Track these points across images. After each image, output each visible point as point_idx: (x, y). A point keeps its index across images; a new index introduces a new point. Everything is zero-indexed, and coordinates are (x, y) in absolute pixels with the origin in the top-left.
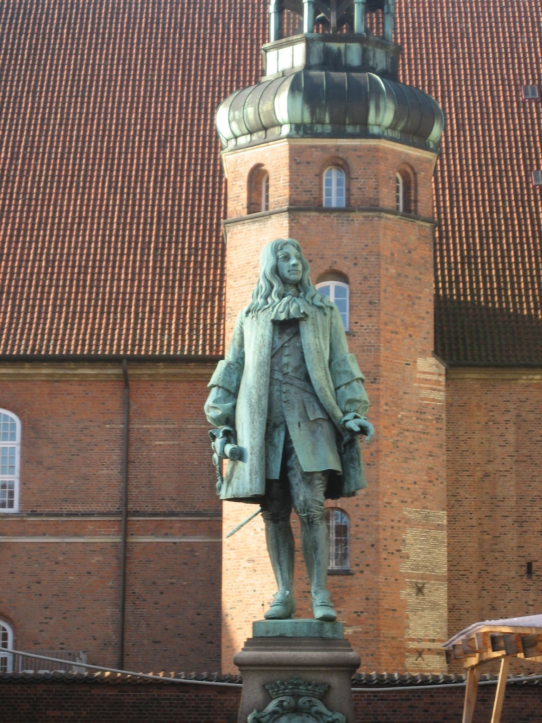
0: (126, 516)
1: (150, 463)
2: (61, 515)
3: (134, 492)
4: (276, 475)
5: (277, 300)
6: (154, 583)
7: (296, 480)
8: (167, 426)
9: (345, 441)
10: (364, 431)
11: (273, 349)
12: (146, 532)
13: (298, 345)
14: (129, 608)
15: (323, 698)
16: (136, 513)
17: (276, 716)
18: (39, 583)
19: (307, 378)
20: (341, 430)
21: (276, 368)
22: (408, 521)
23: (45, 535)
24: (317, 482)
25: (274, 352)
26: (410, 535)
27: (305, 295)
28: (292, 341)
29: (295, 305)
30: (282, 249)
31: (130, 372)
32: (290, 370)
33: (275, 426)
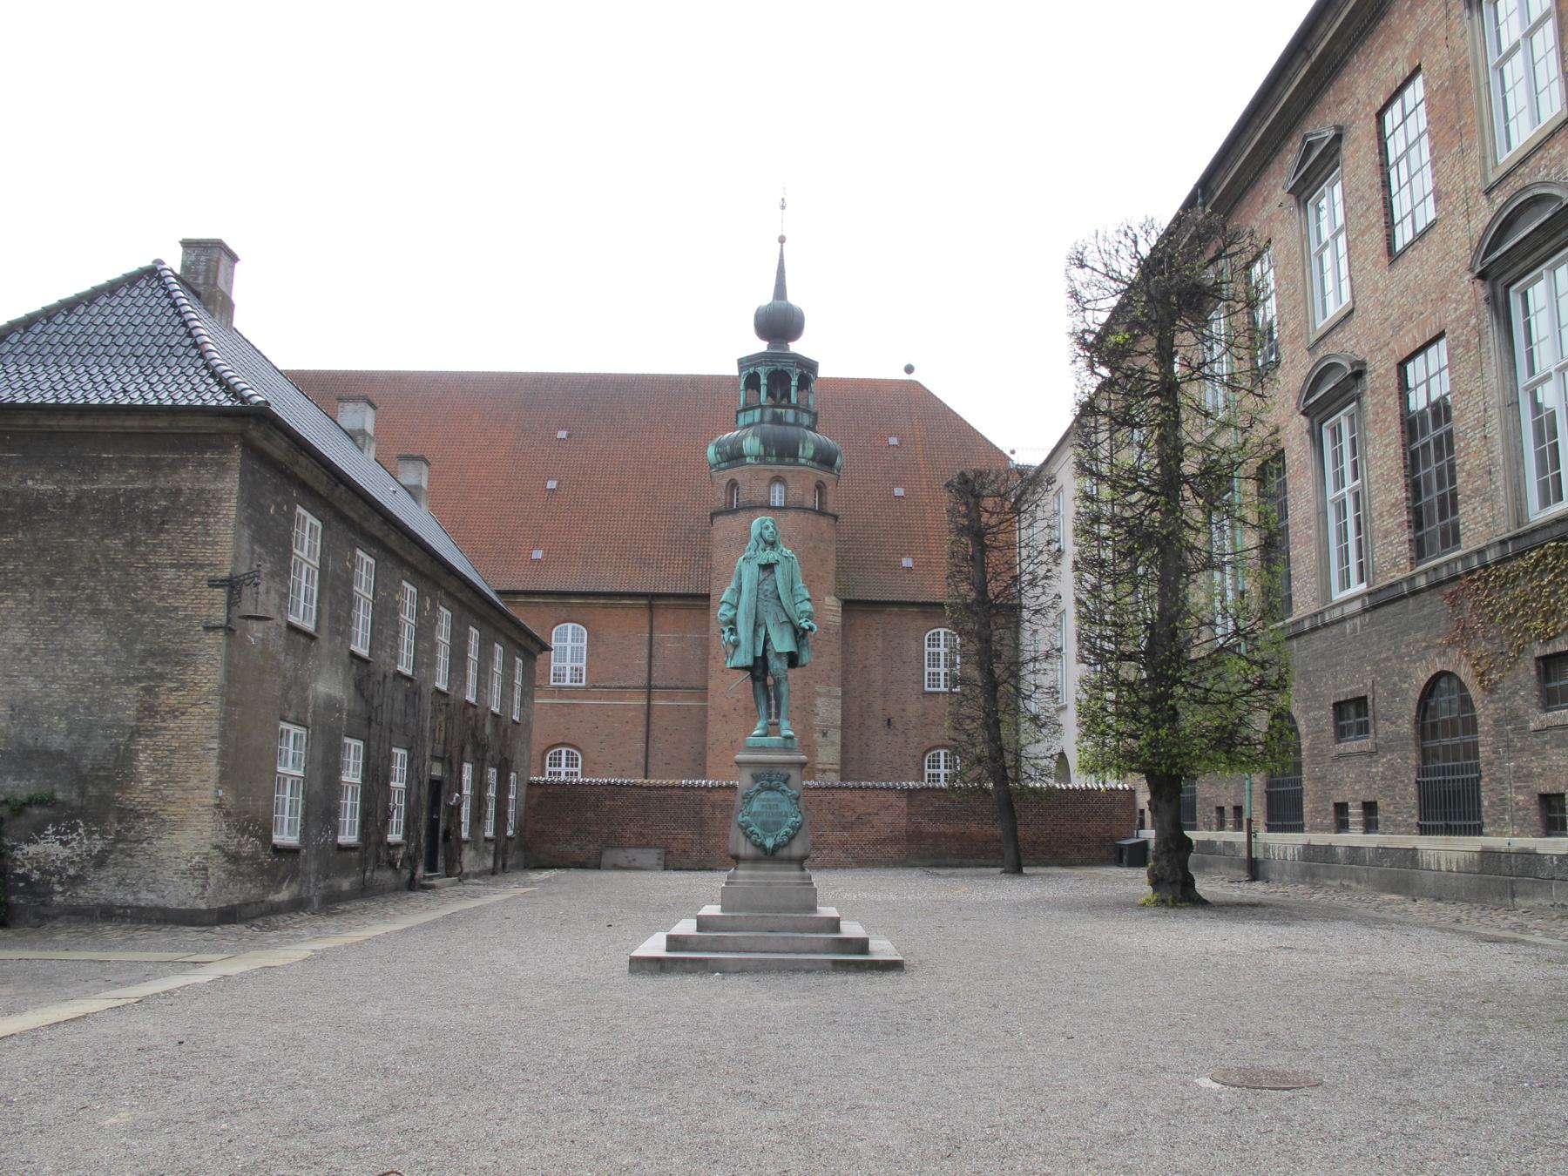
4: (759, 653)
7: (771, 657)
9: (800, 635)
10: (811, 629)
12: (662, 698)
15: (786, 782)
22: (819, 694)
26: (819, 701)
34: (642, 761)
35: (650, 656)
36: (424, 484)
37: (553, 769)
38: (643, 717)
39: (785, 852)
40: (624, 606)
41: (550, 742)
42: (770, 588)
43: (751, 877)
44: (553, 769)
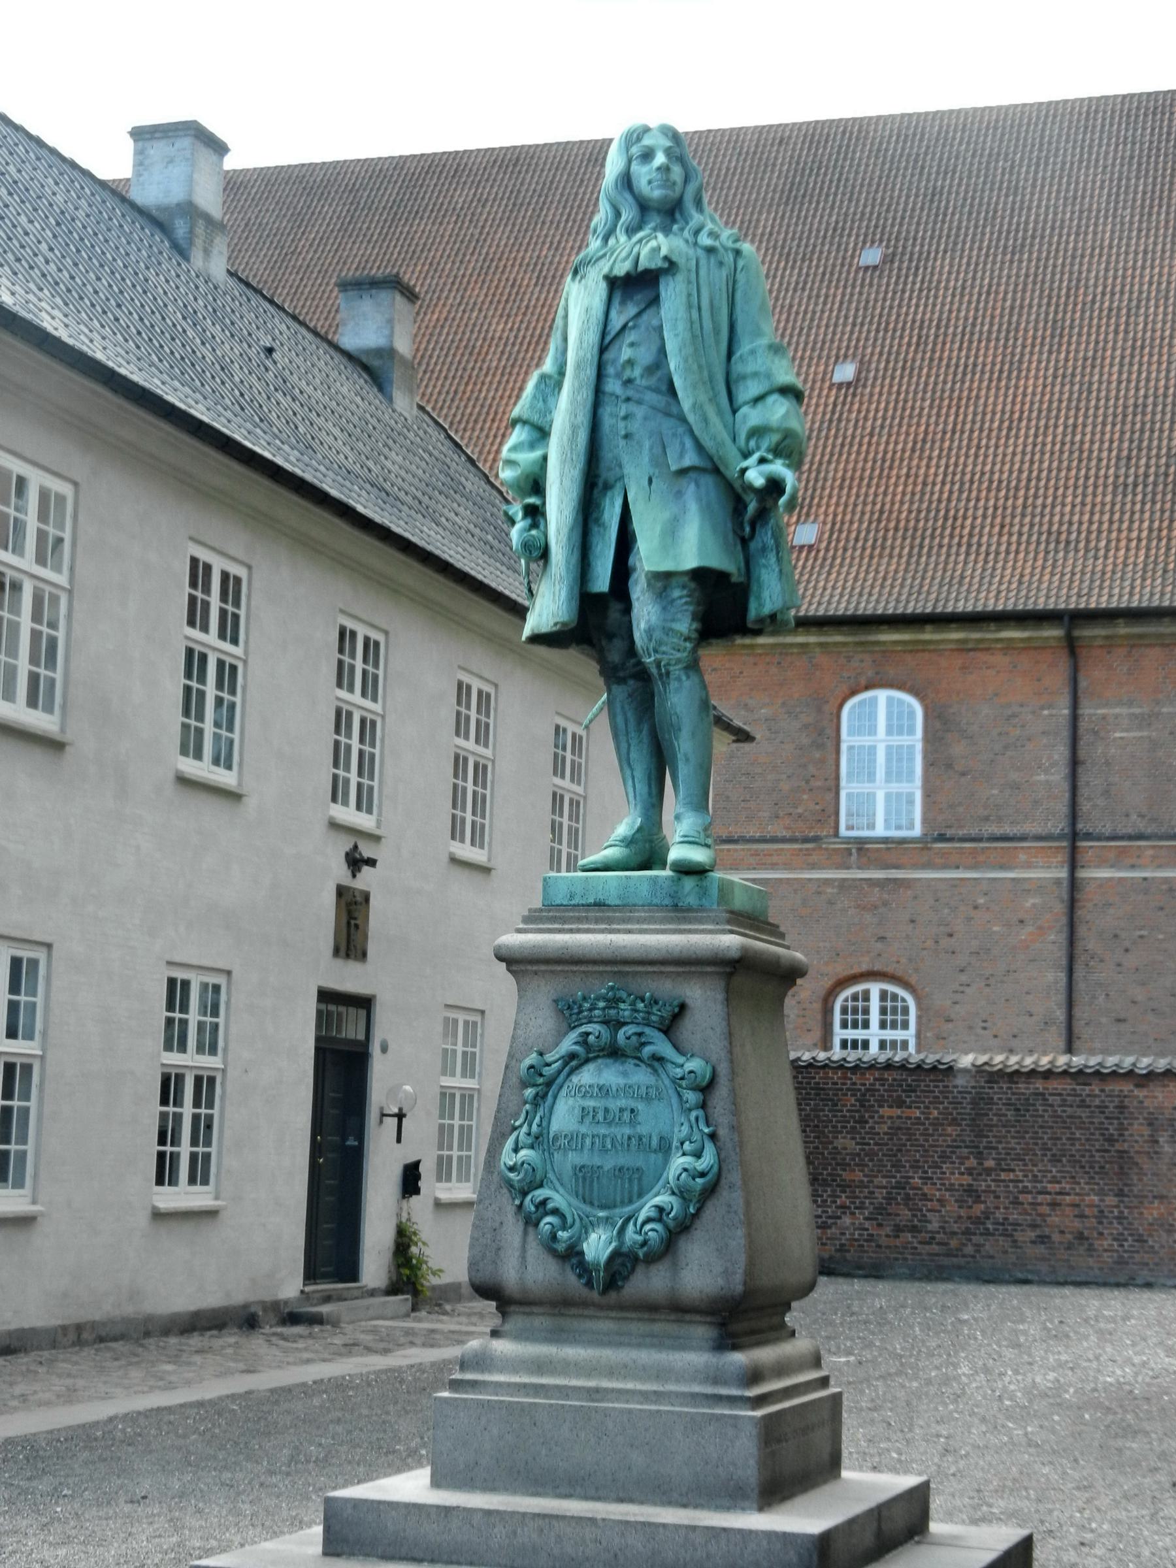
0: (1074, 840)
1: (1107, 763)
2: (980, 840)
3: (1085, 806)
4: (602, 582)
5: (623, 238)
6: (1116, 936)
7: (639, 591)
8: (1132, 710)
9: (749, 514)
10: (775, 486)
11: (604, 334)
12: (1102, 863)
13: (655, 322)
14: (1079, 973)
16: (1089, 836)
17: (574, 1063)
18: (951, 935)
19: (672, 390)
20: (740, 490)
21: (611, 370)
23: (958, 867)
24: (676, 593)
25: (608, 339)
27: (682, 229)
28: (645, 317)
29: (653, 243)
30: (639, 139)
31: (1077, 633)
32: (637, 372)
33: (607, 487)
34: (1060, 1015)
35: (1075, 763)
36: (403, 346)
37: (851, 1034)
38: (1060, 908)
39: (651, 1282)
40: (1009, 646)
41: (842, 970)
42: (645, 356)
43: (539, 1366)
44: (851, 1034)
